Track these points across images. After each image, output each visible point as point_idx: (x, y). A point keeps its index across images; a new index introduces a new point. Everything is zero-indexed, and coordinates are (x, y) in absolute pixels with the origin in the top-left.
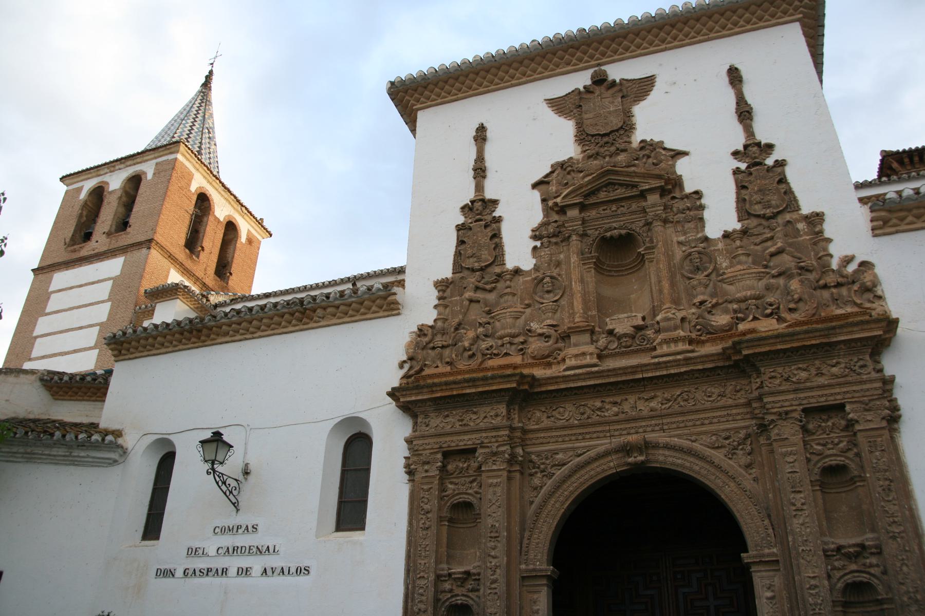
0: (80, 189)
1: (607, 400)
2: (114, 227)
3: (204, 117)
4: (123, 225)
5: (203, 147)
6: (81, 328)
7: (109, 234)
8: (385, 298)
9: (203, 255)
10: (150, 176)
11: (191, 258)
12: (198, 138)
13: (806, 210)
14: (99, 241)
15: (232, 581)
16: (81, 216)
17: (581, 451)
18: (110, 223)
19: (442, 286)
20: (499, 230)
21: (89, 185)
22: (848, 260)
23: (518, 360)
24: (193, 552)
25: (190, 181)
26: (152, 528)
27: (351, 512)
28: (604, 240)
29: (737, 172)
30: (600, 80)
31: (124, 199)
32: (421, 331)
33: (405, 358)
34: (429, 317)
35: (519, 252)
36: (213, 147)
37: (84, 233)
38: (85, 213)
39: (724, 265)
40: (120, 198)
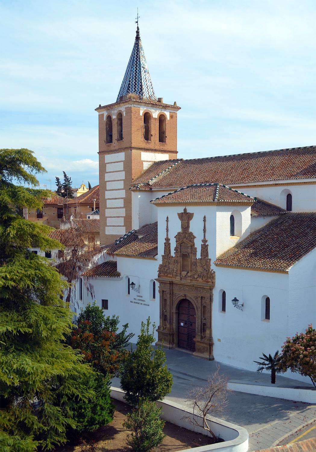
0: (103, 115)
2: (119, 136)
6: (118, 180)
9: (152, 138)
11: (148, 142)
12: (140, 77)
13: (209, 258)
14: (115, 144)
15: (140, 305)
16: (107, 128)
17: (179, 294)
19: (163, 256)
20: (170, 246)
21: (105, 114)
22: (212, 270)
24: (135, 299)
27: (154, 297)
29: (202, 245)
30: (185, 210)
32: (160, 265)
33: (158, 270)
35: (173, 254)
37: (109, 139)
38: (108, 126)
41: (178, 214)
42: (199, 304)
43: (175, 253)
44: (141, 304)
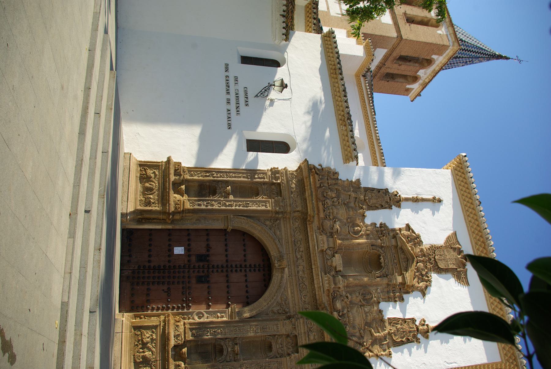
1: (303, 254)
2: (409, 16)
3: (479, 57)
4: (410, 20)
5: (461, 59)
7: (405, 14)
8: (351, 157)
9: (396, 66)
10: (439, 32)
11: (395, 59)
12: (466, 56)
18: (411, 13)
20: (385, 208)
23: (322, 215)
24: (236, 79)
25: (438, 55)
26: (246, 60)
28: (380, 256)
31: (426, 20)
32: (336, 173)
34: (343, 176)
36: (461, 65)
39: (366, 309)
40: (426, 17)
41: (433, 214)
42: (275, 327)
43: (376, 224)
44: (228, 102)
